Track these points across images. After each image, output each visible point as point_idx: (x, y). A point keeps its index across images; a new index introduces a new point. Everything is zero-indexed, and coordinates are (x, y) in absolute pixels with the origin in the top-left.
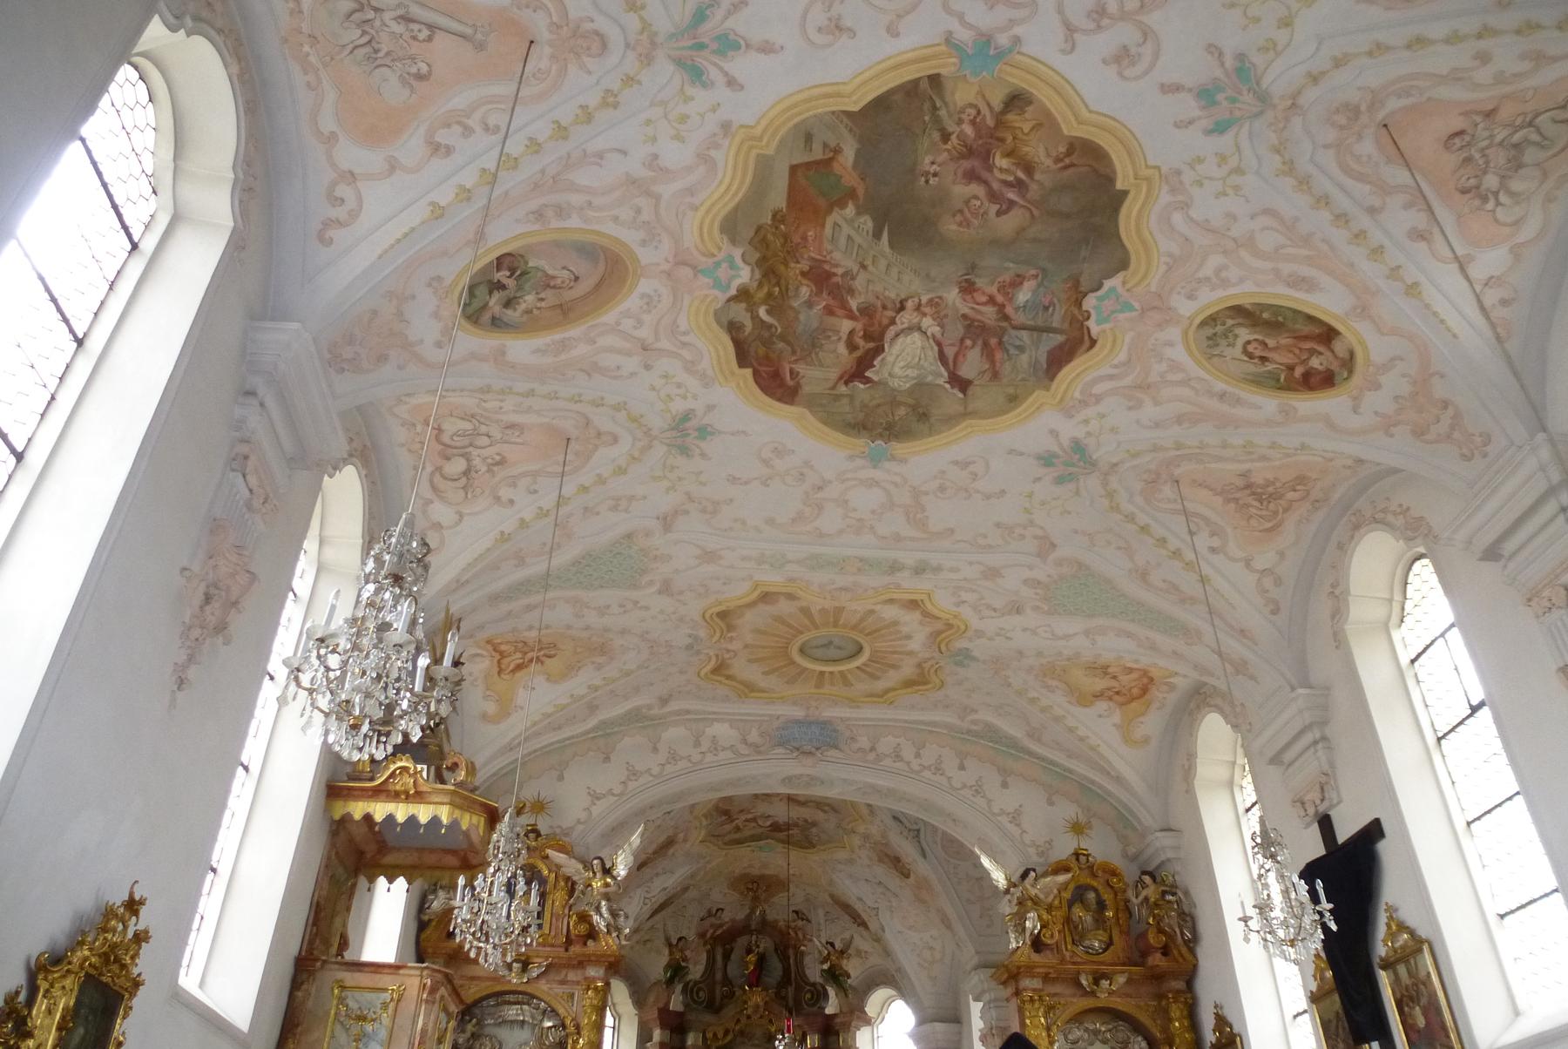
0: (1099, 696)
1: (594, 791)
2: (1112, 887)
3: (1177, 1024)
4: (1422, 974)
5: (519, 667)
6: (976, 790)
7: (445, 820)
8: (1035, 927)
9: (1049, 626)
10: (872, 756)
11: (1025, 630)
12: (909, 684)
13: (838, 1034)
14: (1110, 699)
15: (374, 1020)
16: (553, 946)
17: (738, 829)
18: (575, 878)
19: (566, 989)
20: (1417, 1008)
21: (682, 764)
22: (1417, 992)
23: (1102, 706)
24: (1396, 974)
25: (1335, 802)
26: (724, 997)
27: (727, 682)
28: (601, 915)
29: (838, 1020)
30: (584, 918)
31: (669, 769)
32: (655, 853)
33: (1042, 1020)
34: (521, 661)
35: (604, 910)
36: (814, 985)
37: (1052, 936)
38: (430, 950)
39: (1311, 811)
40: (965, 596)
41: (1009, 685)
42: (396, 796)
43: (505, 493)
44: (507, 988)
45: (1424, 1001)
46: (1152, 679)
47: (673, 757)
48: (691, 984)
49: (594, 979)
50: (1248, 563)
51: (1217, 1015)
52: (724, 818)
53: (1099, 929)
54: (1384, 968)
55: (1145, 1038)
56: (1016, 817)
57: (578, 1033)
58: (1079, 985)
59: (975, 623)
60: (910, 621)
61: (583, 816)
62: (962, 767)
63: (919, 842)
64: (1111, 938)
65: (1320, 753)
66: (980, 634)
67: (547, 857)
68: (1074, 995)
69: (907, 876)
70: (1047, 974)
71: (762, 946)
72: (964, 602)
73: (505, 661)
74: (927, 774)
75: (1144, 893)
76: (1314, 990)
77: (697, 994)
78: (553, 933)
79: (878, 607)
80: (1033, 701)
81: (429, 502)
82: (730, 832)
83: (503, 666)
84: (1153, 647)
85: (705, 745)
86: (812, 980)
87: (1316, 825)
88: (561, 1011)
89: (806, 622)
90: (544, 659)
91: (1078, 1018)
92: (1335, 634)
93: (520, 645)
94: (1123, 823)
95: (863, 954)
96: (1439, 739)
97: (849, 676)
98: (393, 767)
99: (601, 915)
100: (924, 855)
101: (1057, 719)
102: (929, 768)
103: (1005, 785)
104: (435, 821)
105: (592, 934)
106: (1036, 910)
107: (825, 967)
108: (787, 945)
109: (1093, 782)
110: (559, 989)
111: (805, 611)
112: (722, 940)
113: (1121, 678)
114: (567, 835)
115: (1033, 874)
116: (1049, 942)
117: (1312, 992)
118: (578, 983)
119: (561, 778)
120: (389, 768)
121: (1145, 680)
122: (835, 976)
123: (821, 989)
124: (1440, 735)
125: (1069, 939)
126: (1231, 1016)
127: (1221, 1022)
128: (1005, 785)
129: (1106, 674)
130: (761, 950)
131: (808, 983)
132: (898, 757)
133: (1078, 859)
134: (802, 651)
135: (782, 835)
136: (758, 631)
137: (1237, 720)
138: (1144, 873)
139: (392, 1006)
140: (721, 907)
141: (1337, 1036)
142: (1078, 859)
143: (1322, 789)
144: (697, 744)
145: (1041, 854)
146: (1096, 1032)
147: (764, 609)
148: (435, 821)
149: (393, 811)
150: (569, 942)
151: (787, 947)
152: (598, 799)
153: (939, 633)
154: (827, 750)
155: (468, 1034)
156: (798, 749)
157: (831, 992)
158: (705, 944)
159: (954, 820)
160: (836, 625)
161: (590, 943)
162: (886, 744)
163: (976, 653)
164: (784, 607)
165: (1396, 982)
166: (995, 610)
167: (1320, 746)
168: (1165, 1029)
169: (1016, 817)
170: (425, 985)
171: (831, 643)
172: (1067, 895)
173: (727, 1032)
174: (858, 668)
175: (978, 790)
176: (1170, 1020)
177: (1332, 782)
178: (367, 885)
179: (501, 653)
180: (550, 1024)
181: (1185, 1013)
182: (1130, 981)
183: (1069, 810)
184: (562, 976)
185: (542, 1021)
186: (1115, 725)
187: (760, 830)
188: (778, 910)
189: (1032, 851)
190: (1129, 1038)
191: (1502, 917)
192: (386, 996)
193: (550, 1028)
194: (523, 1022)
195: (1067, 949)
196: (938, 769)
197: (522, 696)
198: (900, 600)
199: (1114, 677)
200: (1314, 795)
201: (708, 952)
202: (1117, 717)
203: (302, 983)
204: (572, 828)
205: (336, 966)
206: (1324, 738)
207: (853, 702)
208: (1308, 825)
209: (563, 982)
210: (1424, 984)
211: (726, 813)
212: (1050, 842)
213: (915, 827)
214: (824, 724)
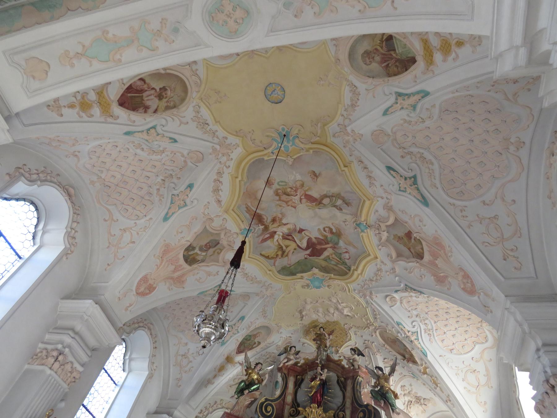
63: (418, 189)
77: (266, 409)
95: (422, 401)
100: (425, 202)
130: (324, 377)
131: (361, 406)
151: (346, 379)
213: (411, 174)
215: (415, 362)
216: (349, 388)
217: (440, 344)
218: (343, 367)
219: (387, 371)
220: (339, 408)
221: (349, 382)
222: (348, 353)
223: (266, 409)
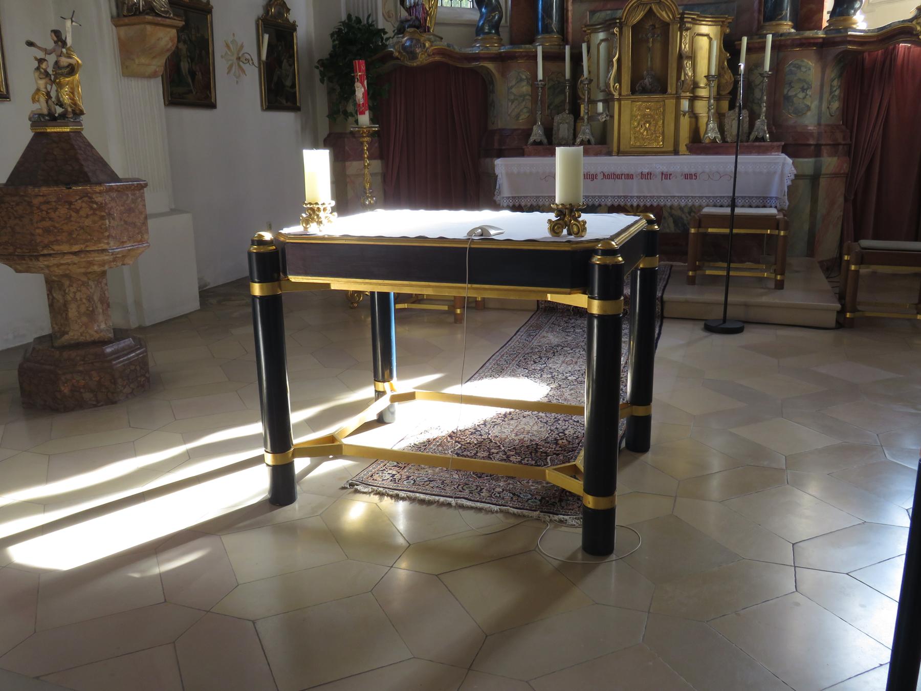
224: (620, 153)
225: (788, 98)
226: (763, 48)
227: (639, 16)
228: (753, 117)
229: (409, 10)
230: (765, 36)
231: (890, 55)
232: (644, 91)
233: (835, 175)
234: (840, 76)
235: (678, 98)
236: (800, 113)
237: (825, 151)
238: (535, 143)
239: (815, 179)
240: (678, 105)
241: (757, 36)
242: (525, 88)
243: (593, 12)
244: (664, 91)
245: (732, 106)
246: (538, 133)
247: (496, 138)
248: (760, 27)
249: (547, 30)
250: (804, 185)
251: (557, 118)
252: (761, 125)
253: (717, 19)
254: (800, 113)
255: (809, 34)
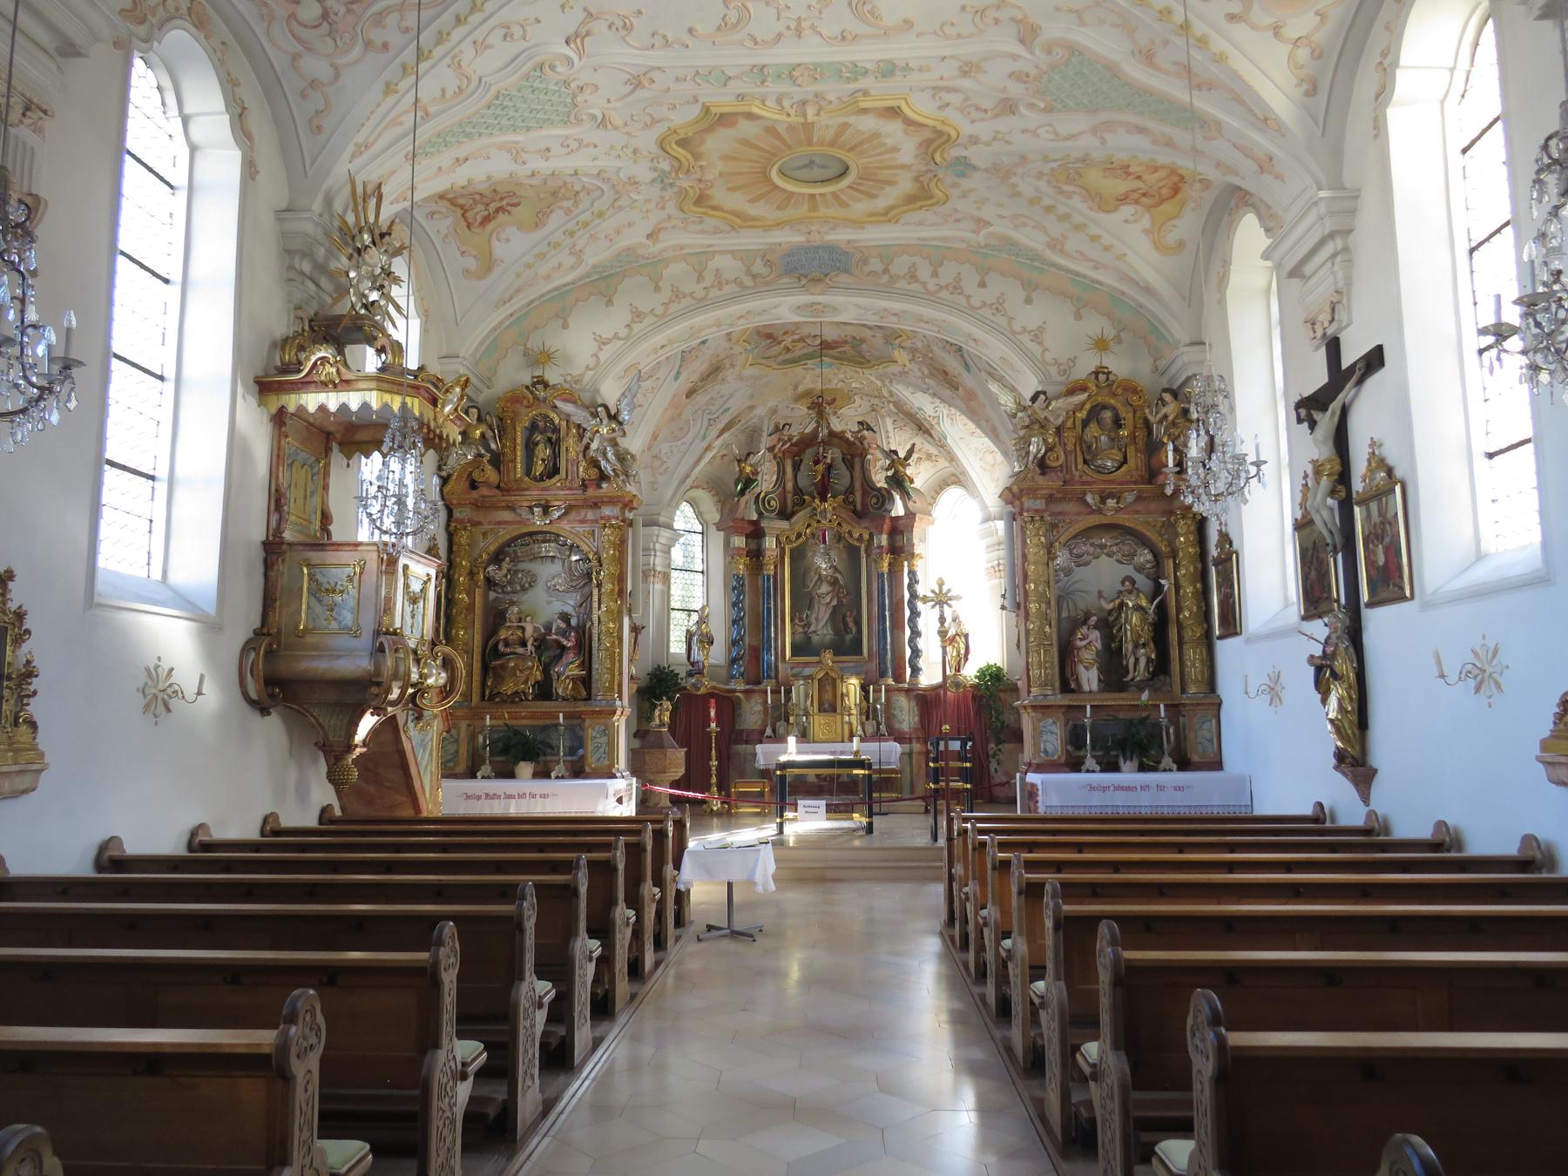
0: (1123, 199)
1: (600, 336)
2: (1131, 405)
3: (1182, 539)
4: (1390, 515)
5: (487, 219)
6: (997, 309)
7: (375, 405)
8: (1039, 451)
9: (1050, 125)
10: (885, 279)
11: (1024, 131)
12: (911, 199)
13: (902, 533)
14: (1137, 202)
15: (342, 592)
16: (570, 489)
17: (788, 350)
18: (584, 426)
19: (586, 528)
20: (1380, 546)
21: (686, 302)
22: (1383, 530)
23: (1127, 210)
24: (1368, 511)
25: (1344, 324)
26: (795, 505)
27: (715, 213)
28: (608, 460)
29: (901, 522)
30: (595, 463)
31: (674, 307)
32: (702, 380)
33: (1043, 539)
34: (486, 213)
35: (610, 455)
36: (880, 489)
37: (1058, 458)
38: (455, 502)
39: (1319, 333)
40: (947, 97)
41: (1018, 194)
42: (325, 385)
43: (377, 36)
44: (531, 529)
45: (1387, 540)
46: (1182, 177)
47: (677, 295)
48: (762, 495)
49: (609, 518)
50: (1277, 30)
51: (1220, 532)
52: (769, 341)
53: (1113, 448)
54: (1359, 504)
55: (1152, 551)
56: (1037, 336)
57: (601, 565)
58: (1086, 504)
59: (966, 129)
60: (893, 130)
61: (592, 362)
62: (983, 285)
63: (962, 356)
64: (1125, 457)
65: (1336, 268)
66: (974, 140)
67: (556, 407)
68: (1079, 514)
69: (957, 389)
70: (1051, 496)
71: (829, 456)
72: (947, 105)
73: (470, 215)
74: (945, 294)
75: (1164, 410)
76: (1299, 518)
77: (769, 503)
78: (570, 478)
79: (852, 119)
80: (1049, 209)
81: (295, 58)
82: (780, 354)
83: (470, 220)
84: (1169, 143)
85: (709, 279)
86: (879, 485)
87: (1324, 349)
88: (584, 547)
89: (776, 142)
90: (509, 208)
91: (1087, 533)
92: (1376, 120)
93: (478, 197)
94: (1149, 335)
96: (1472, 251)
97: (843, 197)
98: (313, 359)
99: (608, 460)
101: (1079, 228)
102: (946, 287)
103: (1028, 301)
104: (365, 406)
105: (603, 477)
106: (1042, 433)
107: (890, 473)
108: (854, 452)
109: (1123, 293)
110: (580, 528)
111: (771, 130)
112: (796, 451)
113: (1146, 177)
114: (576, 382)
115: (1042, 397)
116: (1054, 465)
117: (1296, 520)
118: (596, 521)
119: (565, 326)
120: (309, 360)
121: (1175, 179)
122: (899, 482)
123: (885, 493)
124: (1474, 244)
125: (1080, 460)
126: (1233, 536)
127: (1225, 539)
128: (1028, 301)
129: (1128, 174)
130: (829, 461)
132: (913, 277)
133: (1097, 378)
134: (782, 172)
135: (834, 352)
136: (725, 158)
137: (1270, 222)
138: (1165, 390)
139: (356, 578)
140: (789, 421)
141: (1311, 562)
142: (1097, 378)
143: (1333, 310)
144: (700, 279)
145: (1063, 372)
146: (1102, 547)
147: (724, 133)
148: (365, 406)
149: (324, 401)
150: (584, 486)
151: (853, 456)
152: (605, 344)
153: (928, 143)
154: (837, 275)
155: (505, 571)
156: (806, 277)
157: (897, 497)
158: (775, 457)
159: (975, 340)
160: (810, 143)
161: (604, 485)
162: (900, 265)
163: (975, 162)
164: (746, 128)
165: (1368, 517)
166: (986, 111)
167: (1338, 259)
168: (1170, 543)
169: (1037, 336)
170: (382, 559)
171: (812, 162)
172: (1081, 415)
173: (799, 536)
174: (849, 187)
175: (999, 308)
176: (1177, 535)
177: (1345, 301)
178: (345, 461)
179: (462, 207)
180: (577, 558)
181: (1192, 528)
182: (1139, 498)
183: (1095, 325)
184: (582, 516)
185: (570, 556)
186: (1144, 230)
187: (811, 350)
188: (844, 421)
189: (1053, 370)
190: (1136, 551)
191: (1491, 456)
192: (349, 570)
193: (577, 561)
194: (553, 557)
195: (1077, 469)
196: (956, 288)
197: (499, 249)
198: (875, 108)
199: (1139, 178)
200: (1324, 317)
201: (778, 464)
202: (1146, 222)
203: (273, 564)
204: (582, 375)
205: (301, 548)
206: (1346, 249)
207: (859, 224)
208: (1317, 348)
209: (583, 521)
210: (1390, 524)
211: (769, 336)
212: (1073, 360)
214: (832, 249)
215: (931, 435)
216: (857, 467)
217: (961, 427)
218: (847, 441)
219: (902, 455)
220: (847, 490)
221: (857, 461)
222: (855, 428)
223: (769, 503)
224: (814, 742)
225: (894, 715)
226: (881, 691)
227: (821, 675)
228: (879, 724)
229: (693, 664)
230: (880, 686)
231: (938, 695)
232: (825, 711)
233: (919, 753)
234: (917, 704)
235: (843, 715)
236: (900, 722)
237: (914, 741)
238: (767, 737)
239: (910, 754)
240: (842, 718)
241: (876, 683)
242: (760, 708)
243: (792, 669)
244: (835, 711)
245: (868, 719)
246: (769, 731)
247: (745, 734)
248: (877, 681)
249: (769, 677)
250: (906, 758)
251: (778, 724)
252: (883, 727)
253: (857, 674)
254: (900, 722)
255: (900, 685)
